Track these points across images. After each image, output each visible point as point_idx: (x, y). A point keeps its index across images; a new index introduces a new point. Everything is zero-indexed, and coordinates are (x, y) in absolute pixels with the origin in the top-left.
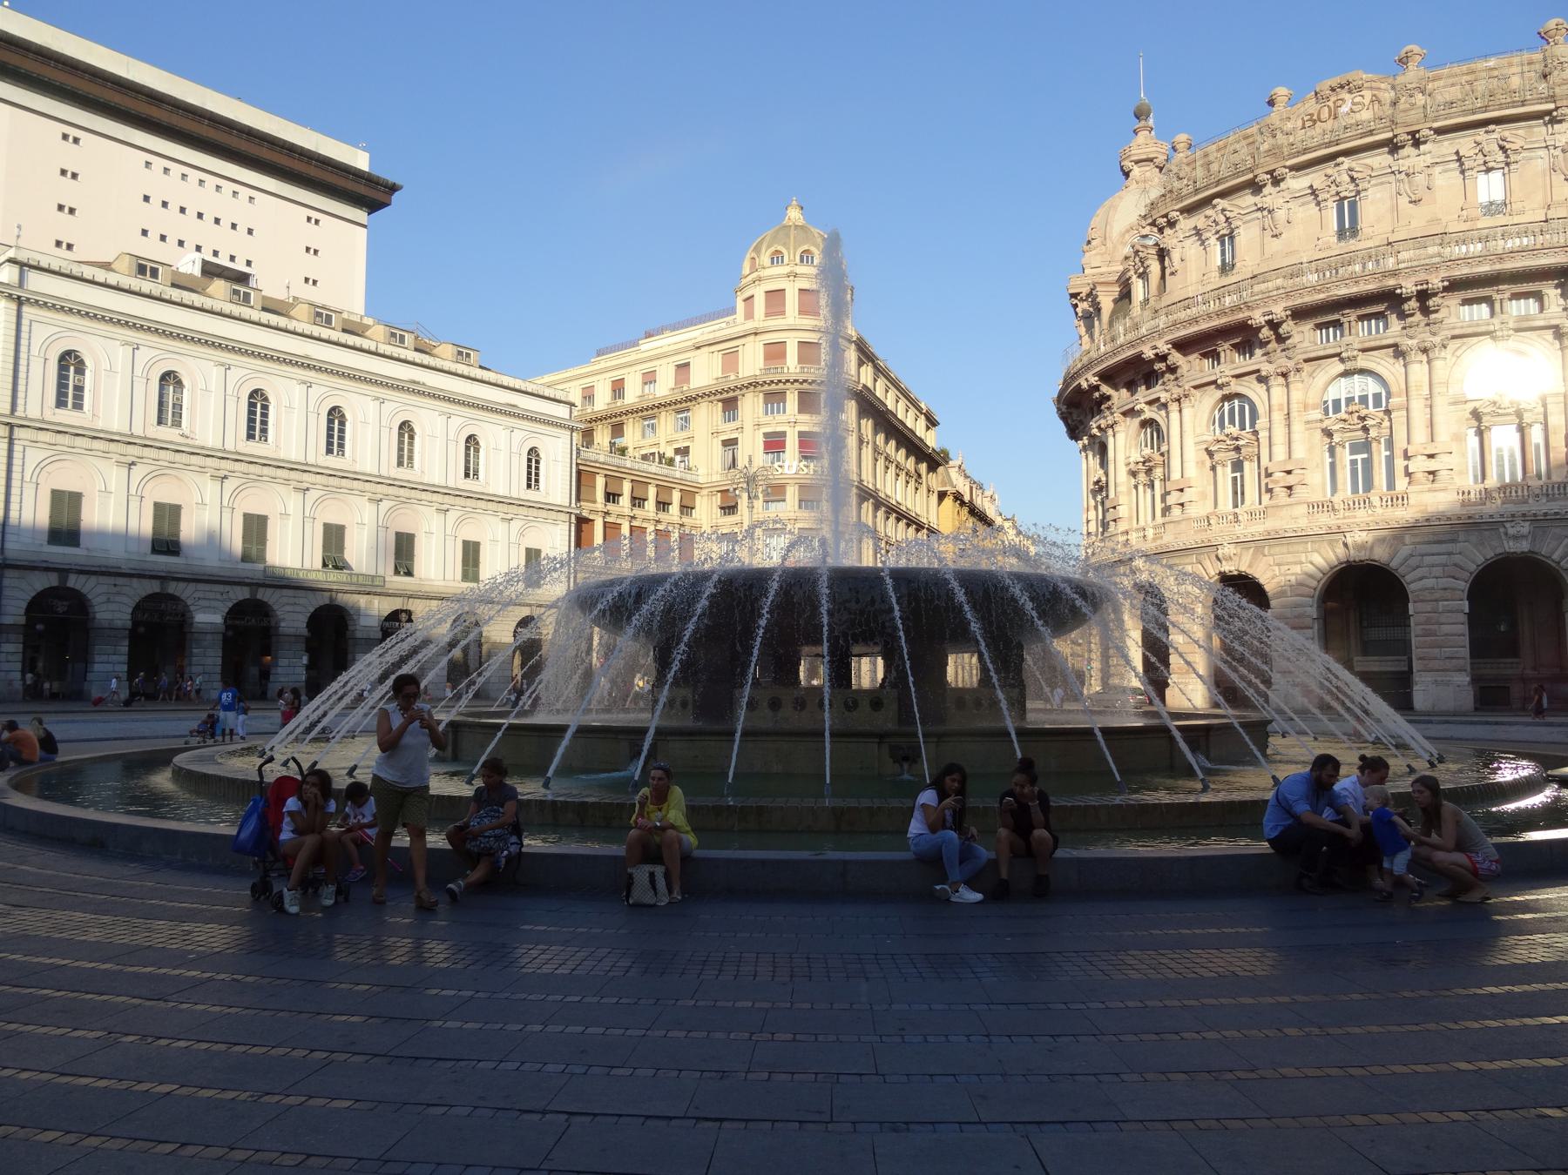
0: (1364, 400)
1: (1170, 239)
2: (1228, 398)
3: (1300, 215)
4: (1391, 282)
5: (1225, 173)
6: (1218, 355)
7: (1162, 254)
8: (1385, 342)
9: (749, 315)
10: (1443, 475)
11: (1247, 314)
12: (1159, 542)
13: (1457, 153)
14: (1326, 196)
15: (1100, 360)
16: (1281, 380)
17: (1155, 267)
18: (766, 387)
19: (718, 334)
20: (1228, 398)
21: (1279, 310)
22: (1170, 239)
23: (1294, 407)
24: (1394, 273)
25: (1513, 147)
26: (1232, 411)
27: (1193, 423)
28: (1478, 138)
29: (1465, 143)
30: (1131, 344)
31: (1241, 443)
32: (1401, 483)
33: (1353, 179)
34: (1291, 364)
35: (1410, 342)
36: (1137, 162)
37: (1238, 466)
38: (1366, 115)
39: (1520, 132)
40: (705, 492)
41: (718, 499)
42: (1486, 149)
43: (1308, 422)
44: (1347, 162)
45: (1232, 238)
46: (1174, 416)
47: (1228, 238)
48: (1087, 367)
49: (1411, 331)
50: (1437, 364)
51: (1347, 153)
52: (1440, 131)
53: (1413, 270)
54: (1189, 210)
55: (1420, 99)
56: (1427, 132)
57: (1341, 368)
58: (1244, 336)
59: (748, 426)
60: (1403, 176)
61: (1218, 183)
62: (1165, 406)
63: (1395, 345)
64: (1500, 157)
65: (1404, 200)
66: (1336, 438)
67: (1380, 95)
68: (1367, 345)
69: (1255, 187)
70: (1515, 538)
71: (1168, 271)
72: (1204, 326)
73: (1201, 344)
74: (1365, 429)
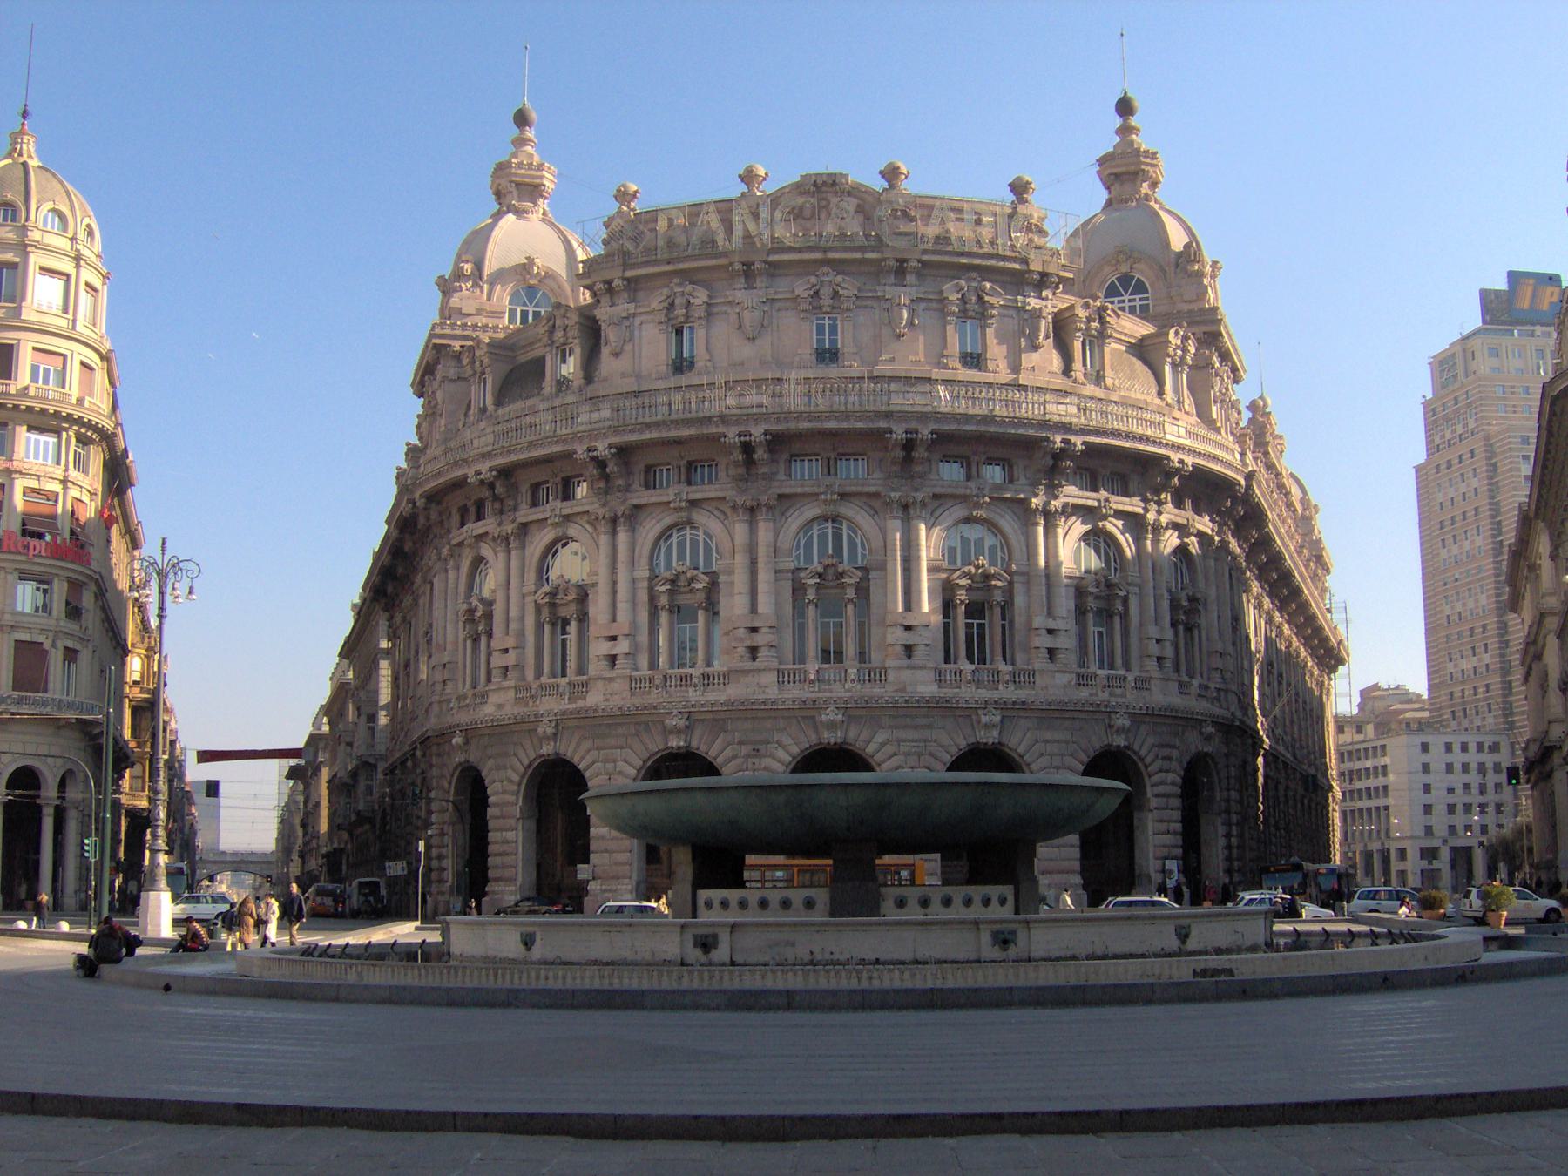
4: (882, 424)
8: (866, 489)
10: (919, 652)
11: (721, 429)
12: (580, 704)
13: (941, 292)
14: (808, 307)
21: (757, 432)
23: (762, 552)
24: (888, 415)
26: (681, 545)
31: (698, 586)
32: (876, 657)
36: (518, 184)
44: (830, 276)
48: (485, 456)
52: (924, 264)
53: (903, 416)
56: (914, 264)
63: (876, 495)
68: (848, 489)
70: (987, 726)
71: (605, 352)
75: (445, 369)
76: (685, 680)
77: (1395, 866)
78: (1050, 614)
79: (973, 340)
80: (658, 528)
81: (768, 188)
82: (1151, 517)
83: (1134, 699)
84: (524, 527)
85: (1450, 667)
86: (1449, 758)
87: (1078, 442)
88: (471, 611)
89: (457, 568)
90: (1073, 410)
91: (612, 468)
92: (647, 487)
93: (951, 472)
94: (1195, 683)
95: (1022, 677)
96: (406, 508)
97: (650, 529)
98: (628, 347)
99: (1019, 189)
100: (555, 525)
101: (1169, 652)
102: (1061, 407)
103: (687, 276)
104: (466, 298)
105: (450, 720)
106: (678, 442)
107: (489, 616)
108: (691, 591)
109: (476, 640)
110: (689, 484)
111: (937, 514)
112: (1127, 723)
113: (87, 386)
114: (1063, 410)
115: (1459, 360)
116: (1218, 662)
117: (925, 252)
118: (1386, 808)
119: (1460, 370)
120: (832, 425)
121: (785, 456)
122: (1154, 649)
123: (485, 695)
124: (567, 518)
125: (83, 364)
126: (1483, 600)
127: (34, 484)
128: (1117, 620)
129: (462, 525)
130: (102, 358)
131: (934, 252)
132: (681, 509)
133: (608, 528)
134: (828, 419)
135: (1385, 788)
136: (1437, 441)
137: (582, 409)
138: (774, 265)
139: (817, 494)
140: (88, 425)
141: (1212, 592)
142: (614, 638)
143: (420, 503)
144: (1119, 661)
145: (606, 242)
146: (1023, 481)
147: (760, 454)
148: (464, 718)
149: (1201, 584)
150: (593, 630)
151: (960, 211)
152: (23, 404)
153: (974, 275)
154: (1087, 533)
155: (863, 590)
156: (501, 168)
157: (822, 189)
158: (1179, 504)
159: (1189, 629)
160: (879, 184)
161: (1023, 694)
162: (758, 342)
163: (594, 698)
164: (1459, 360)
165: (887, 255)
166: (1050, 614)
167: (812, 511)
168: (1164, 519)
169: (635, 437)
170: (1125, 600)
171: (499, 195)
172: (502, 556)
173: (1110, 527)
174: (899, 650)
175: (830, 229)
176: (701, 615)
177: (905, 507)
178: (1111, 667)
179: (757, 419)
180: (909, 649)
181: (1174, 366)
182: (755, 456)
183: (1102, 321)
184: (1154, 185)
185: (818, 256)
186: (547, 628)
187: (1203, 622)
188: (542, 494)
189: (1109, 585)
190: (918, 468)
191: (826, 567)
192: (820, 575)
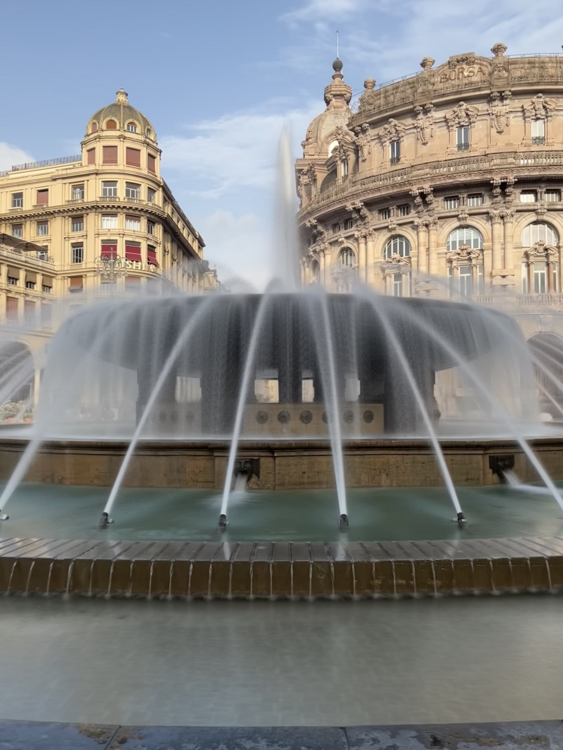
0: (469, 242)
1: (362, 140)
2: (394, 237)
3: (438, 133)
4: (489, 176)
5: (396, 104)
6: (389, 212)
7: (357, 150)
8: (482, 211)
9: (92, 160)
11: (408, 188)
13: (522, 107)
14: (453, 123)
15: (318, 210)
16: (424, 228)
17: (352, 157)
18: (104, 210)
19: (69, 171)
20: (394, 237)
23: (433, 244)
24: (490, 171)
25: (551, 107)
26: (395, 245)
27: (372, 251)
28: (534, 100)
29: (526, 102)
30: (340, 201)
31: (401, 263)
33: (467, 115)
34: (431, 219)
35: (495, 212)
36: (335, 96)
37: (398, 277)
38: (475, 79)
39: (553, 100)
40: (59, 277)
42: (537, 107)
43: (439, 254)
44: (465, 105)
45: (398, 143)
46: (362, 246)
47: (396, 143)
48: (310, 214)
49: (495, 206)
50: (509, 225)
51: (466, 100)
53: (500, 170)
54: (374, 124)
57: (457, 224)
58: (403, 201)
59: (91, 235)
60: (494, 117)
61: (394, 108)
62: (357, 240)
63: (487, 213)
64: (543, 112)
65: (494, 131)
66: (455, 263)
67: (484, 68)
68: (473, 211)
69: (413, 114)
71: (360, 160)
72: (384, 193)
73: (381, 205)
74: (470, 260)
81: (435, 67)
93: (528, 199)
98: (370, 156)
104: (311, 150)
111: (518, 220)
121: (442, 198)
125: (149, 188)
130: (159, 186)
131: (520, 85)
133: (362, 241)
139: (457, 216)
140: (150, 213)
147: (430, 198)
151: (534, 63)
153: (540, 95)
156: (327, 90)
162: (428, 144)
165: (492, 91)
167: (455, 223)
169: (371, 196)
171: (328, 102)
175: (466, 81)
182: (427, 199)
191: (463, 250)
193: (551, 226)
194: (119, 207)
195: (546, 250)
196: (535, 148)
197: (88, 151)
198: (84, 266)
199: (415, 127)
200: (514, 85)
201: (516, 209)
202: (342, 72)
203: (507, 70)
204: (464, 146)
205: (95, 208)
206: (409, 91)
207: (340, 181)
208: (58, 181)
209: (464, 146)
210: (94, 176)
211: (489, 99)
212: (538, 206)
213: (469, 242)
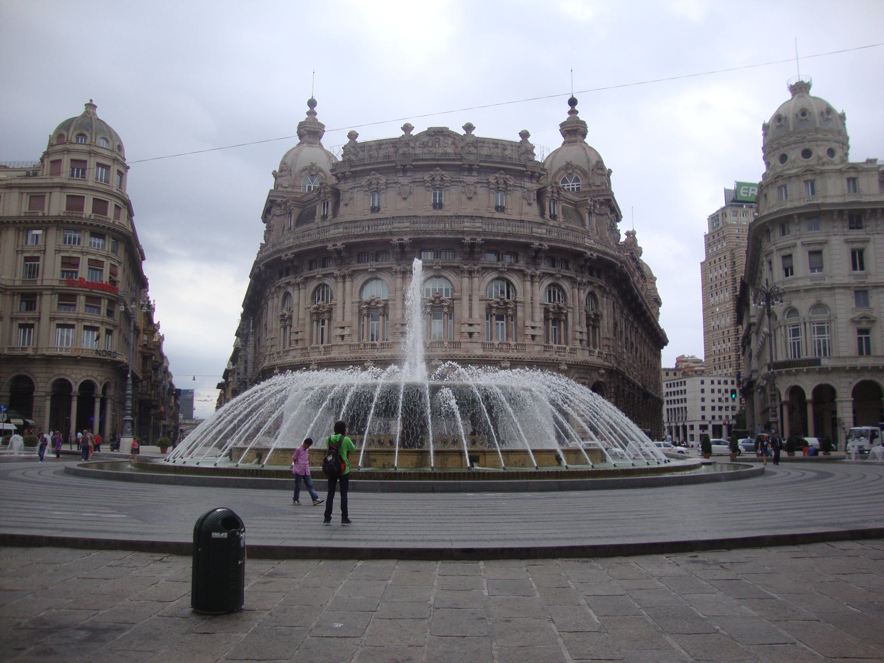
0: (441, 290)
4: (460, 236)
10: (476, 335)
12: (328, 356)
22: (343, 186)
24: (463, 232)
30: (322, 241)
31: (379, 305)
40: (9, 292)
41: (17, 299)
48: (289, 248)
50: (476, 280)
51: (440, 166)
52: (481, 167)
53: (469, 233)
55: (472, 149)
63: (458, 267)
65: (464, 197)
71: (342, 204)
72: (366, 239)
75: (276, 211)
76: (373, 346)
77: (689, 432)
78: (533, 320)
79: (502, 201)
80: (363, 280)
81: (414, 133)
82: (579, 279)
83: (569, 358)
84: (307, 280)
85: (714, 348)
86: (713, 387)
87: (546, 245)
88: (283, 316)
89: (278, 297)
90: (544, 231)
91: (344, 254)
92: (359, 262)
93: (491, 258)
94: (596, 351)
95: (520, 347)
96: (256, 270)
97: (360, 280)
99: (525, 135)
100: (319, 279)
101: (585, 337)
102: (539, 231)
103: (377, 170)
105: (273, 363)
106: (372, 243)
107: (290, 318)
108: (377, 308)
109: (285, 328)
110: (377, 261)
112: (566, 368)
113: (117, 216)
114: (541, 231)
115: (720, 217)
116: (606, 342)
117: (481, 161)
118: (686, 408)
119: (720, 222)
120: (438, 236)
122: (578, 336)
123: (288, 351)
124: (325, 276)
125: (116, 206)
126: (728, 320)
127: (93, 257)
128: (562, 323)
129: (280, 278)
131: (485, 162)
132: (372, 272)
134: (437, 234)
135: (685, 399)
136: (710, 251)
137: (331, 228)
138: (415, 167)
141: (605, 312)
142: (343, 328)
143: (262, 268)
144: (563, 341)
145: (343, 156)
146: (522, 262)
147: (407, 249)
148: (279, 362)
149: (600, 309)
150: (334, 324)
152: (89, 222)
154: (549, 285)
155: (451, 308)
156: (301, 125)
157: (438, 134)
158: (591, 274)
159: (594, 328)
160: (462, 132)
161: (519, 355)
163: (334, 354)
164: (720, 217)
166: (533, 320)
168: (584, 280)
170: (566, 315)
171: (301, 136)
172: (296, 292)
173: (562, 284)
174: (466, 334)
175: (441, 151)
176: (381, 318)
177: (470, 272)
178: (560, 343)
179: (406, 233)
180: (471, 334)
181: (590, 213)
183: (558, 193)
184: (584, 135)
185: (435, 163)
186: (315, 323)
187: (601, 325)
188: (314, 265)
189: (560, 308)
190: (476, 256)
192: (432, 302)
193: (509, 284)
194: (85, 224)
195: (506, 303)
196: (497, 215)
197: (52, 162)
198: (39, 283)
199: (396, 183)
200: (481, 161)
201: (481, 265)
202: (316, 109)
203: (476, 148)
204: (438, 205)
205: (60, 224)
206: (392, 150)
207: (318, 218)
208: (13, 190)
209: (438, 205)
210: (59, 190)
211: (460, 169)
212: (500, 265)
213: (441, 290)
